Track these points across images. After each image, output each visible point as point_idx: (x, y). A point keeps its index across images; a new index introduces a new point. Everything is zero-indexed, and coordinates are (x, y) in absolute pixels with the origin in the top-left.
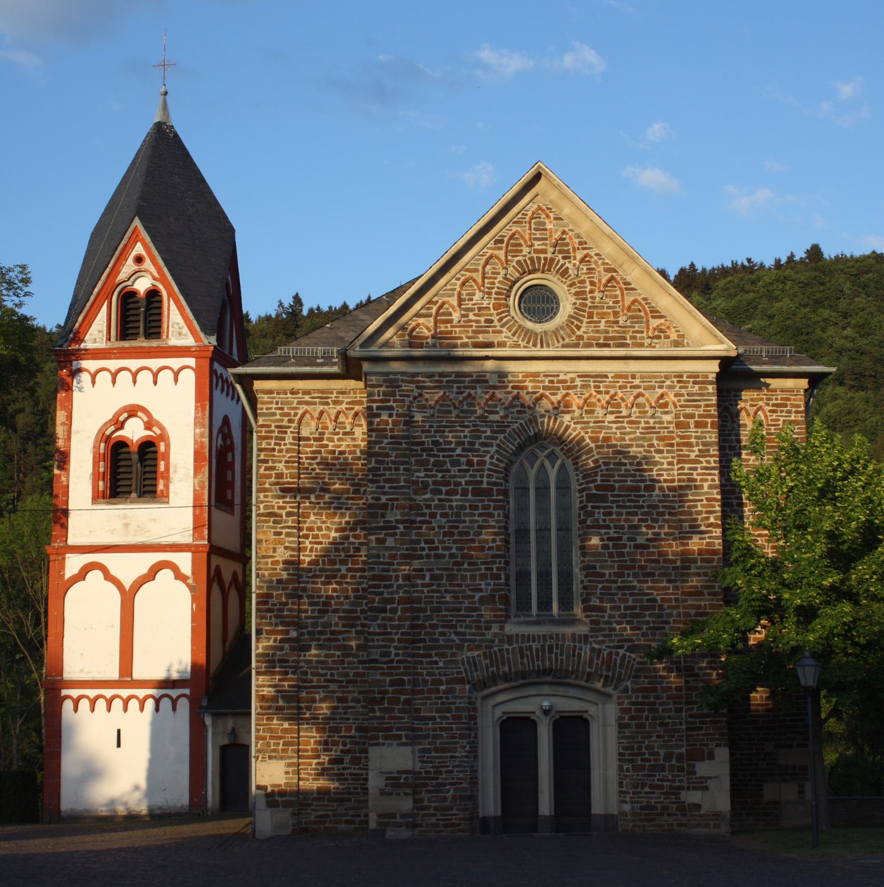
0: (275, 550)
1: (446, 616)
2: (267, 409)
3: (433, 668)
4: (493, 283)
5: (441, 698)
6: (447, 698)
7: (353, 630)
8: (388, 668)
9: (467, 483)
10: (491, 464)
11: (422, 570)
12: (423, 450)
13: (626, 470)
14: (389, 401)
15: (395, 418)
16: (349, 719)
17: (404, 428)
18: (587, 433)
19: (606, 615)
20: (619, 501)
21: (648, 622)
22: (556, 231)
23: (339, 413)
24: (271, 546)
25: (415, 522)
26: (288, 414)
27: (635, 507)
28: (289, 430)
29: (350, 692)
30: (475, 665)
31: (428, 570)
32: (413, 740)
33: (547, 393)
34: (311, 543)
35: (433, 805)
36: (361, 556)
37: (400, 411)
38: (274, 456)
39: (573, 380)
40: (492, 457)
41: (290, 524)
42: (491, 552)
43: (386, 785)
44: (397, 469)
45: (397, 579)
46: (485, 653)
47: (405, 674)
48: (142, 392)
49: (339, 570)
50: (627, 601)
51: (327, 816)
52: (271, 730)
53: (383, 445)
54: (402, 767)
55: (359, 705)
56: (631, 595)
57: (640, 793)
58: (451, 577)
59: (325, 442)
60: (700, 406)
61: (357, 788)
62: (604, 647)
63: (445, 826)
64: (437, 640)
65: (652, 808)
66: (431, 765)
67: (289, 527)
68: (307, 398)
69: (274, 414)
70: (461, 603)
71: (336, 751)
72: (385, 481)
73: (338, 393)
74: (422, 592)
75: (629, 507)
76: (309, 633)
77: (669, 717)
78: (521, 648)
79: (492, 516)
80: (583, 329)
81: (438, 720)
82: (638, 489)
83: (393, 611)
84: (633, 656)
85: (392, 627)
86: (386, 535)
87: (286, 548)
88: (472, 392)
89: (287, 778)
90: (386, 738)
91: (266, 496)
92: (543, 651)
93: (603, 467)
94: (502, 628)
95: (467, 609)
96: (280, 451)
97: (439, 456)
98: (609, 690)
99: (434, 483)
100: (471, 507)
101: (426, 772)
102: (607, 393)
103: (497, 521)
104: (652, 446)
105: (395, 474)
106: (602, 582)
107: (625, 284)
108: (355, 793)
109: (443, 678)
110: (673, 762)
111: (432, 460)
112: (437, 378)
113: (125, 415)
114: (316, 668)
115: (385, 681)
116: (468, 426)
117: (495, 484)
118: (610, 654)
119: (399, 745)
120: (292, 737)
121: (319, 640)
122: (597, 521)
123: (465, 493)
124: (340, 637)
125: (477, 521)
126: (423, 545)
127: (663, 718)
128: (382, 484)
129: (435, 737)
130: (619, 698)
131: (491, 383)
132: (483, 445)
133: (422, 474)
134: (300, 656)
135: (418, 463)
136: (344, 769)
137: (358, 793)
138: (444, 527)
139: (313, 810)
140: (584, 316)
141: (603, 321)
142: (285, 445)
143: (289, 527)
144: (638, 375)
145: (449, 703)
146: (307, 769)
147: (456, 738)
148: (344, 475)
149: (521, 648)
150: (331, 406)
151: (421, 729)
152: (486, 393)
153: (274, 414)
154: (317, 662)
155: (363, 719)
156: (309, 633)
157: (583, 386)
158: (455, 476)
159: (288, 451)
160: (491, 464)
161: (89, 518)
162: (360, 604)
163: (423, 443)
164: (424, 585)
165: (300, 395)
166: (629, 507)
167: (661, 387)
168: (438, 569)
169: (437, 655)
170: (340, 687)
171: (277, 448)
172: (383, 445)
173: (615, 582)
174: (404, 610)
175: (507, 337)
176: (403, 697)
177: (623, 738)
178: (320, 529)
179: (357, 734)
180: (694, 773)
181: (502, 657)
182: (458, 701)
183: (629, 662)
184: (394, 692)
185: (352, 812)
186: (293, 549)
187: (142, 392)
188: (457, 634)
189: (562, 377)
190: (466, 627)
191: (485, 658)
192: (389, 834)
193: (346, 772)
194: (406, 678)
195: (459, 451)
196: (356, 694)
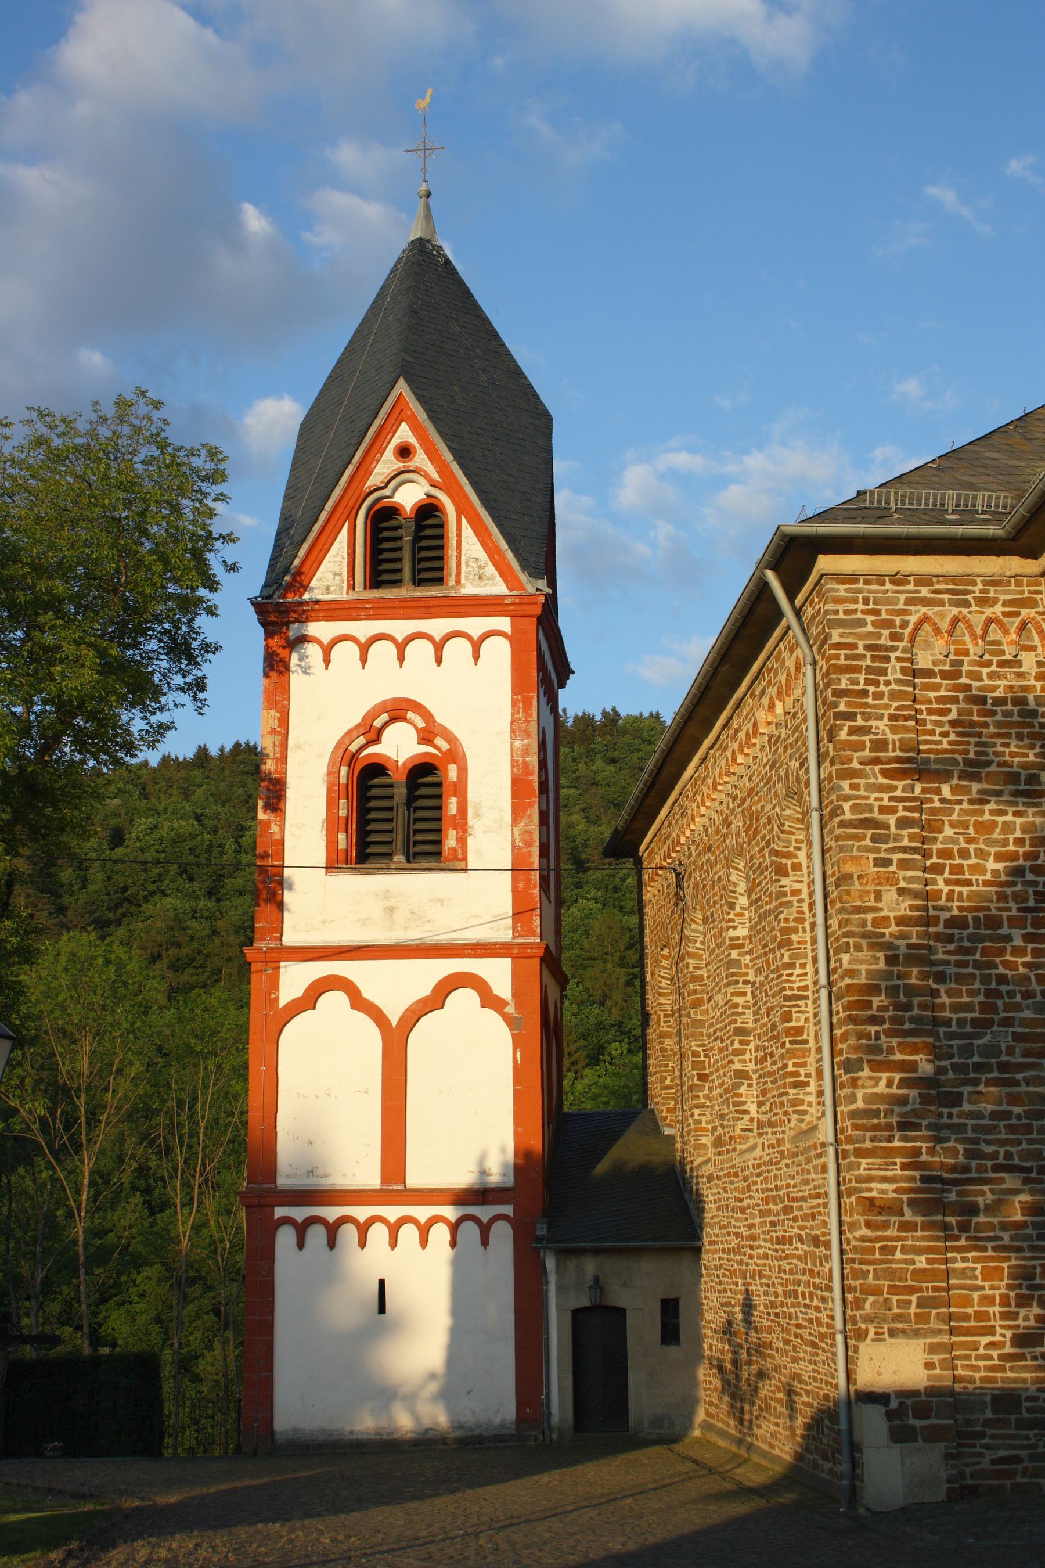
0: (878, 897)
2: (846, 612)
23: (989, 621)
24: (871, 887)
26: (889, 624)
28: (893, 656)
34: (947, 882)
38: (866, 705)
41: (906, 842)
48: (417, 677)
51: (1017, 1460)
52: (890, 1274)
59: (964, 680)
67: (904, 849)
68: (925, 592)
69: (862, 623)
71: (1026, 1318)
87: (901, 891)
91: (853, 787)
96: (879, 696)
113: (385, 717)
114: (975, 1141)
120: (935, 1289)
124: (1019, 1076)
139: (987, 1447)
142: (887, 683)
143: (904, 849)
146: (967, 1357)
150: (974, 608)
153: (862, 623)
154: (976, 1128)
159: (894, 695)
161: (321, 900)
171: (871, 689)
178: (964, 854)
186: (916, 895)
187: (417, 677)
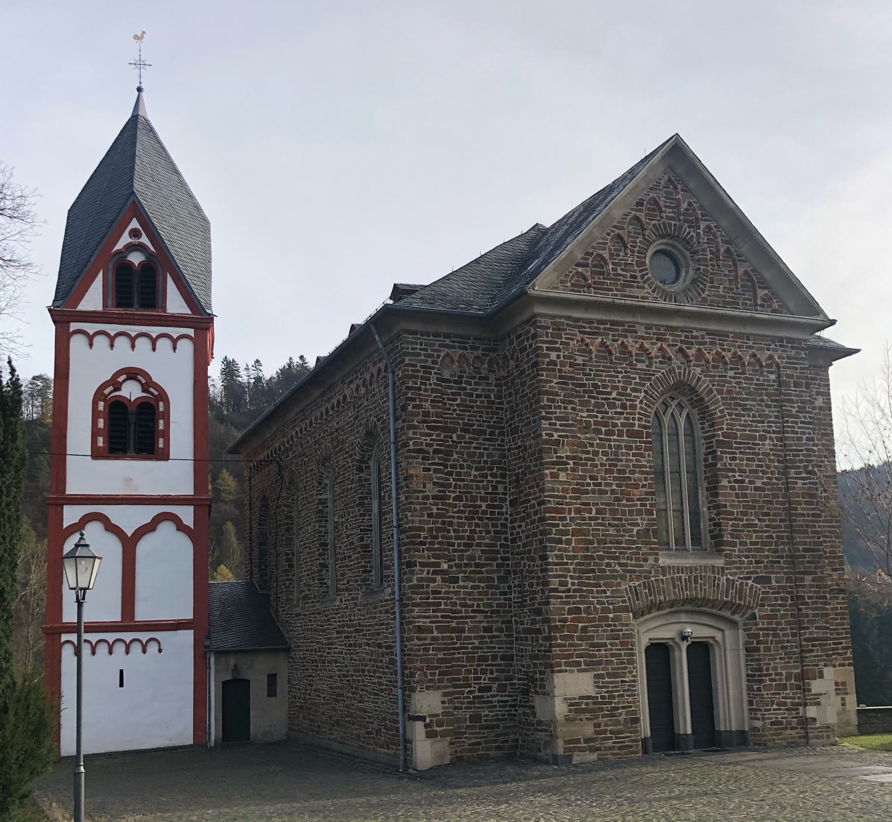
0: (424, 487)
1: (610, 548)
2: (412, 349)
3: (602, 597)
4: (635, 242)
5: (610, 625)
6: (615, 625)
7: (495, 563)
8: (567, 597)
9: (623, 425)
10: (641, 408)
11: (589, 504)
12: (584, 392)
13: (745, 421)
14: (556, 343)
15: (562, 359)
16: (494, 648)
17: (571, 369)
18: (714, 385)
19: (737, 549)
20: (741, 448)
21: (767, 557)
22: (684, 201)
23: (476, 357)
24: (421, 481)
25: (581, 459)
26: (431, 356)
27: (753, 454)
28: (433, 371)
29: (494, 622)
30: (637, 594)
31: (594, 504)
32: (591, 665)
33: (684, 346)
34: (454, 480)
35: (609, 728)
36: (498, 494)
37: (566, 353)
38: (420, 395)
39: (703, 337)
40: (641, 402)
41: (437, 461)
42: (644, 490)
43: (570, 711)
44: (565, 408)
45: (570, 513)
46: (644, 583)
47: (581, 603)
49: (480, 506)
50: (751, 537)
51: (479, 743)
52: (427, 661)
53: (553, 384)
54: (585, 694)
55: (503, 634)
56: (755, 531)
57: (770, 710)
58: (614, 512)
59: (464, 385)
60: (796, 369)
61: (504, 715)
62: (736, 578)
63: (620, 748)
64: (604, 571)
65: (781, 723)
66: (605, 690)
67: (437, 464)
68: (447, 341)
69: (419, 355)
70: (622, 536)
71: (485, 679)
72: (557, 418)
73: (474, 339)
74: (590, 525)
75: (749, 454)
76: (457, 566)
77: (788, 641)
78: (673, 578)
79: (642, 456)
80: (706, 293)
81: (609, 647)
82: (754, 438)
83: (568, 542)
84: (758, 586)
85: (568, 557)
86: (559, 470)
87: (435, 484)
88: (625, 340)
89: (443, 708)
90: (568, 664)
91: (414, 433)
92: (690, 581)
93: (728, 417)
94: (656, 560)
95: (627, 542)
96: (426, 390)
97: (598, 398)
98: (736, 617)
99: (596, 423)
100: (627, 447)
101: (602, 697)
102: (729, 351)
103: (648, 461)
104: (762, 400)
105: (564, 413)
106: (731, 520)
107: (738, 256)
108: (504, 720)
109: (611, 607)
110: (793, 681)
111: (593, 401)
112: (595, 325)
114: (464, 599)
115: (564, 609)
116: (621, 372)
117: (645, 427)
118: (742, 584)
119: (579, 671)
120: (446, 667)
121: (465, 572)
122: (725, 464)
123: (620, 434)
124: (483, 570)
125: (632, 460)
126: (588, 481)
127: (783, 642)
128: (554, 421)
129: (608, 663)
130: (745, 624)
131: (639, 334)
132: (635, 390)
133: (585, 415)
134: (450, 587)
135: (582, 403)
136: (492, 696)
137: (506, 720)
138: (605, 465)
139: (466, 738)
140: (706, 281)
141: (722, 287)
142: (430, 385)
143: (437, 464)
144: (751, 338)
145: (617, 631)
146: (460, 698)
147: (624, 663)
148: (481, 417)
149: (673, 578)
150: (469, 351)
151: (595, 656)
152: (636, 342)
153: (419, 355)
154: (464, 593)
155: (507, 648)
156: (457, 566)
157: (712, 343)
158: (613, 418)
159: (433, 391)
160: (641, 408)
162: (499, 539)
163: (584, 385)
164: (590, 519)
165: (442, 339)
166: (749, 454)
167: (768, 349)
168: (602, 504)
169: (605, 584)
170: (485, 617)
171: (423, 387)
172: (553, 384)
173: (742, 520)
174: (578, 542)
175: (649, 293)
176: (580, 625)
177: (751, 660)
178: (462, 467)
179: (502, 662)
180: (810, 690)
181: (658, 587)
182: (624, 628)
183: (756, 591)
184: (572, 620)
185: (501, 738)
186: (441, 485)
188: (620, 565)
189: (695, 333)
190: (628, 558)
191: (645, 588)
192: (577, 758)
193: (494, 699)
194: (582, 606)
195: (614, 395)
196: (499, 624)
